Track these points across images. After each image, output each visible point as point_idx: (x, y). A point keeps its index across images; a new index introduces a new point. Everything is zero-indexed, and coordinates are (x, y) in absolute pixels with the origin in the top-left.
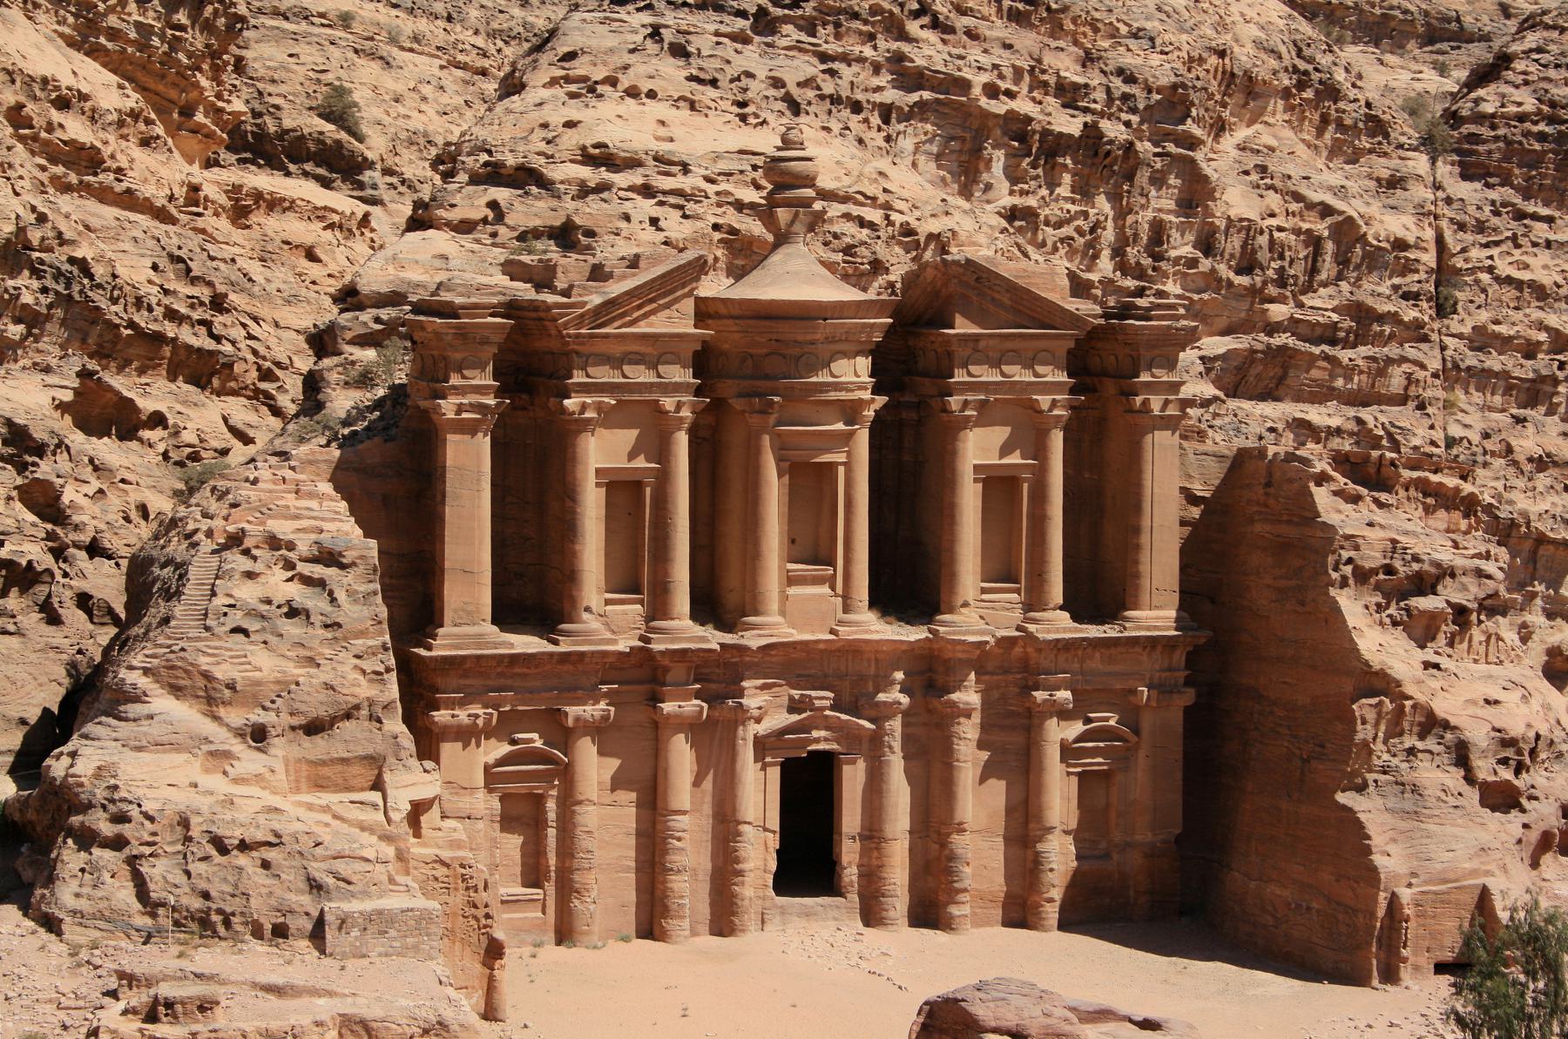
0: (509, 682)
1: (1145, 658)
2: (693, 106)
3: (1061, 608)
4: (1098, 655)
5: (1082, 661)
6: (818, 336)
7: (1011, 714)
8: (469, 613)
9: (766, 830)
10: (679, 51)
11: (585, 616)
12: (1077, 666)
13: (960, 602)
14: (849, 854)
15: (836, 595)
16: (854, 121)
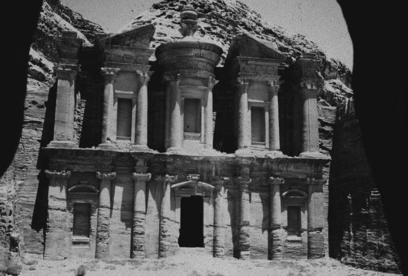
0: (77, 161)
1: (309, 168)
2: (172, 27)
3: (279, 150)
4: (292, 166)
5: (287, 168)
6: (192, 54)
7: (264, 186)
8: (63, 136)
9: (176, 222)
10: (170, 17)
11: (108, 141)
12: (285, 169)
13: (244, 145)
14: (207, 231)
15: (202, 143)
16: (221, 39)
